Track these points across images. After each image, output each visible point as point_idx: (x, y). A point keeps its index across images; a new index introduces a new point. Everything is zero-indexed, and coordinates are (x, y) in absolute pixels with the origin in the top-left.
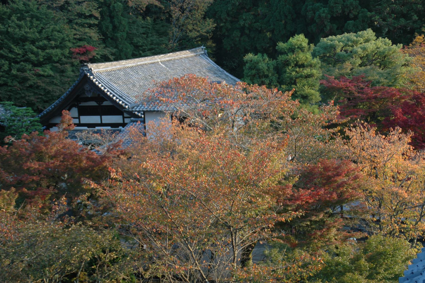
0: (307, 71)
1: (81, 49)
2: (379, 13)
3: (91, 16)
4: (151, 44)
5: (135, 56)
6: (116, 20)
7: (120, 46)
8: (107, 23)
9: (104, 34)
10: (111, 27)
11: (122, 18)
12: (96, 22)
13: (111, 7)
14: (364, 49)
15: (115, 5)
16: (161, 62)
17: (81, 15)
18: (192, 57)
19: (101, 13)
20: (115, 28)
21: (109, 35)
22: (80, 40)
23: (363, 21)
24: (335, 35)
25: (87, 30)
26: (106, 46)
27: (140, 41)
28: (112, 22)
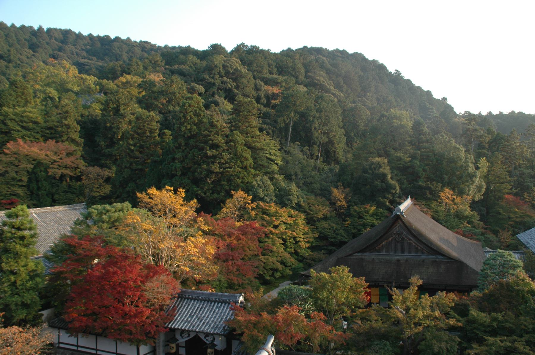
0: (20, 233)
1: (9, 201)
2: (202, 189)
3: (21, 180)
4: (66, 199)
5: (52, 205)
6: (40, 183)
7: (41, 200)
8: (34, 185)
9: (32, 192)
10: (36, 187)
11: (44, 182)
12: (25, 184)
13: (37, 175)
14: (110, 217)
15: (40, 174)
16: (35, 213)
17: (13, 179)
18: (65, 210)
19: (29, 178)
20: (39, 189)
21: (35, 192)
22: (11, 195)
23: (192, 193)
24: (110, 204)
25: (16, 189)
26: (31, 200)
27: (56, 197)
28: (37, 184)
